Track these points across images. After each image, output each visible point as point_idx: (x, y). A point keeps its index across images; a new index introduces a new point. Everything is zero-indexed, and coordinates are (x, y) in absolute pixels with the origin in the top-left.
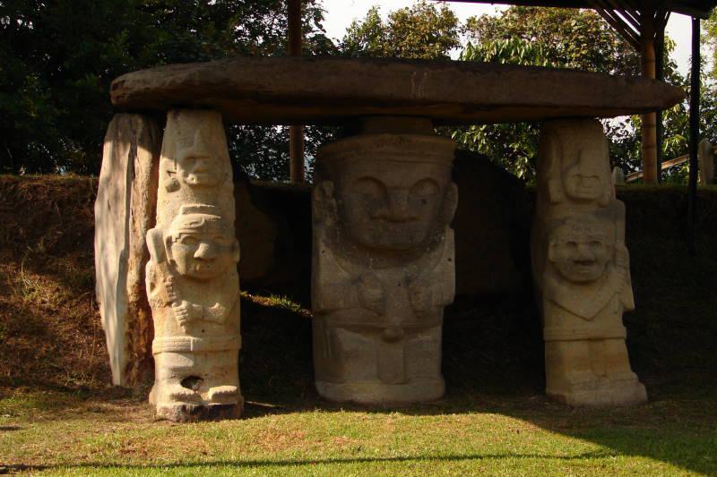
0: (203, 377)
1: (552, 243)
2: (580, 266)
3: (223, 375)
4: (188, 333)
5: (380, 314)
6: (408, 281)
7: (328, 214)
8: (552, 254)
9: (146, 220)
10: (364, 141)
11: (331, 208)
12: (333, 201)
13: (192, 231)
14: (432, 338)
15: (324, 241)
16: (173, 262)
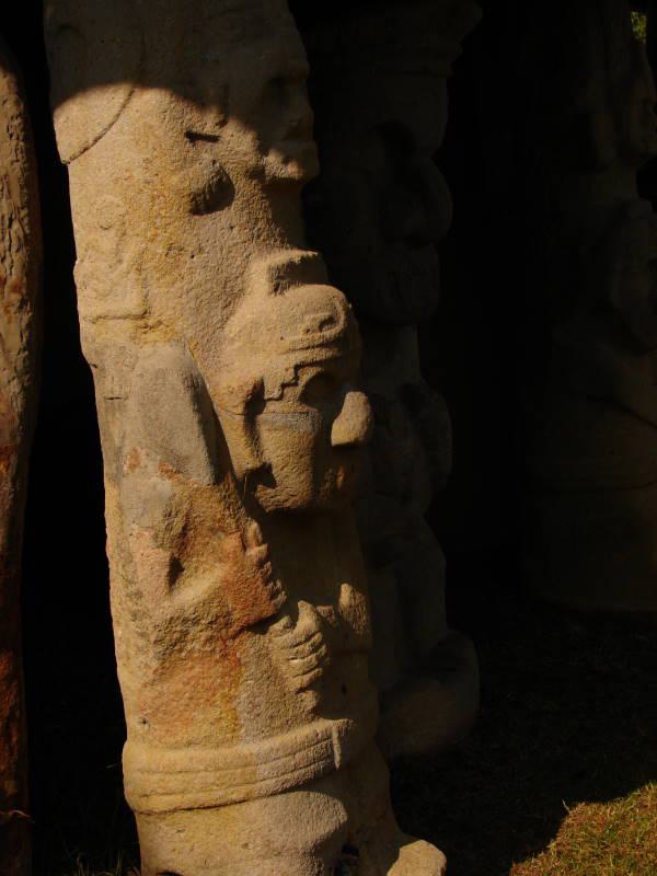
4: (318, 712)
9: (26, 318)
13: (323, 354)
16: (263, 474)
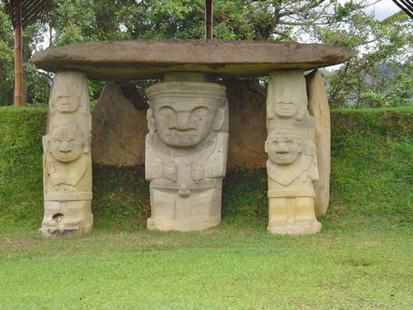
2: (280, 155)
5: (175, 182)
6: (192, 163)
10: (162, 85)
14: (210, 196)
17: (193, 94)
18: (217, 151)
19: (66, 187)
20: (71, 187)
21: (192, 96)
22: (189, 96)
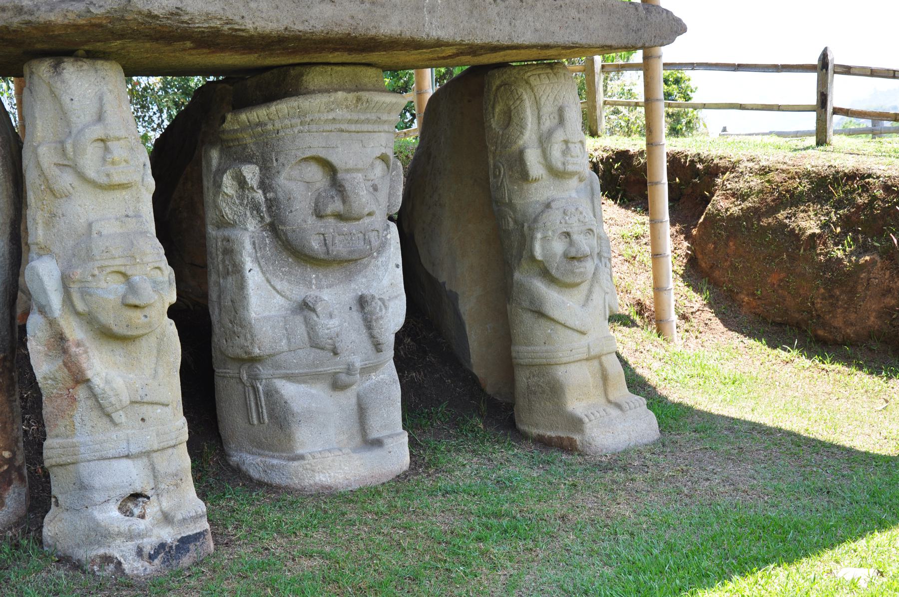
0: (149, 493)
1: (539, 235)
3: (177, 485)
7: (248, 213)
8: (538, 253)
11: (256, 207)
12: (259, 195)
15: (250, 256)
17: (375, 122)
18: (394, 266)
19: (146, 410)
20: (159, 410)
21: (370, 127)
22: (365, 127)
